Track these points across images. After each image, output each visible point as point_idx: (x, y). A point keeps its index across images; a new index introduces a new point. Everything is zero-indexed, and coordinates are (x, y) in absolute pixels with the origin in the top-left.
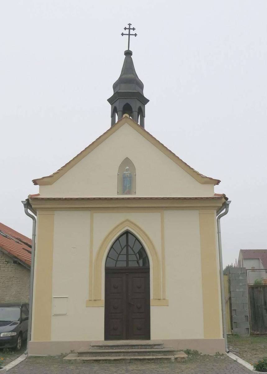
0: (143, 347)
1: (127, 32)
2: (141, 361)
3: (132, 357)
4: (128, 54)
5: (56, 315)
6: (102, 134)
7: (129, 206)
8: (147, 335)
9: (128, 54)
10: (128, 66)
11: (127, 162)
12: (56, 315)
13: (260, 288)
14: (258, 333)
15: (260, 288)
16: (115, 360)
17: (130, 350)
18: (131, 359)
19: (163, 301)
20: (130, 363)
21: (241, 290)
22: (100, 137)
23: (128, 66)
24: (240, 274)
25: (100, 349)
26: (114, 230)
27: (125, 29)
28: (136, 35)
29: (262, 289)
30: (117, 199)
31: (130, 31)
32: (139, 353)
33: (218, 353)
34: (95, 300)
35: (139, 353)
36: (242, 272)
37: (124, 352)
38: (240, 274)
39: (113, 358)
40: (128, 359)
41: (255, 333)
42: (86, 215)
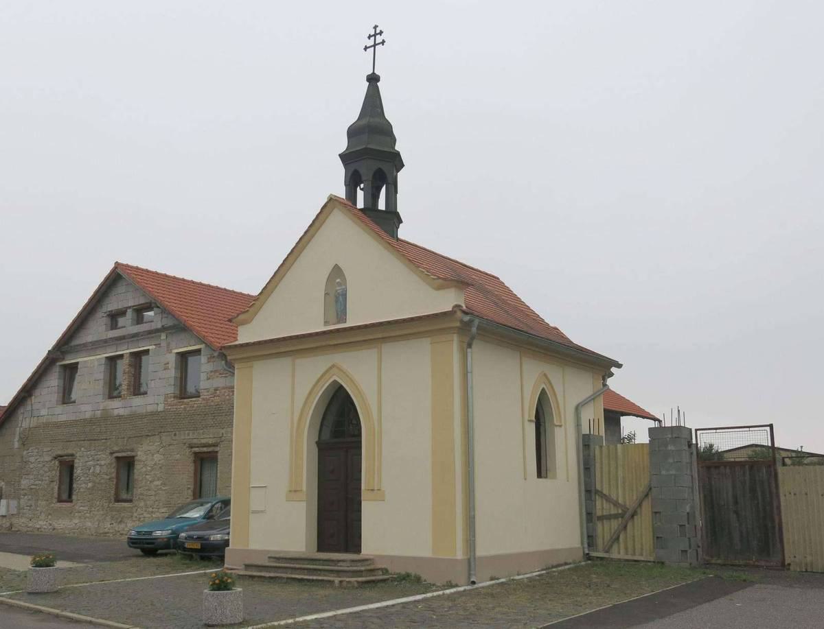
0: (325, 563)
1: (371, 42)
2: (299, 582)
3: (290, 576)
4: (373, 79)
5: (254, 512)
6: (302, 234)
7: (371, 337)
8: (357, 548)
9: (373, 79)
10: (373, 101)
11: (337, 271)
12: (254, 512)
13: (725, 467)
14: (719, 561)
15: (725, 467)
16: (271, 578)
17: (298, 566)
18: (288, 578)
19: (379, 494)
20: (286, 583)
21: (671, 472)
22: (301, 239)
23: (373, 101)
24: (668, 439)
25: (276, 562)
26: (315, 386)
27: (370, 37)
28: (383, 42)
29: (728, 470)
30: (324, 333)
31: (376, 38)
32: (310, 571)
33: (450, 582)
34: (295, 491)
35: (310, 571)
36: (674, 436)
37: (292, 568)
38: (668, 439)
39: (267, 575)
40: (284, 578)
41: (713, 561)
42: (285, 362)
